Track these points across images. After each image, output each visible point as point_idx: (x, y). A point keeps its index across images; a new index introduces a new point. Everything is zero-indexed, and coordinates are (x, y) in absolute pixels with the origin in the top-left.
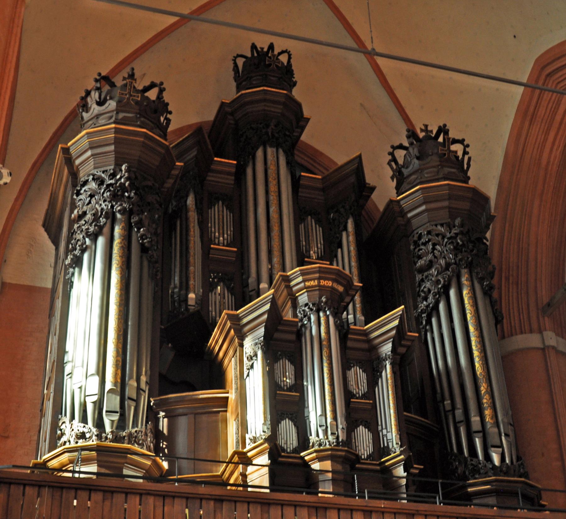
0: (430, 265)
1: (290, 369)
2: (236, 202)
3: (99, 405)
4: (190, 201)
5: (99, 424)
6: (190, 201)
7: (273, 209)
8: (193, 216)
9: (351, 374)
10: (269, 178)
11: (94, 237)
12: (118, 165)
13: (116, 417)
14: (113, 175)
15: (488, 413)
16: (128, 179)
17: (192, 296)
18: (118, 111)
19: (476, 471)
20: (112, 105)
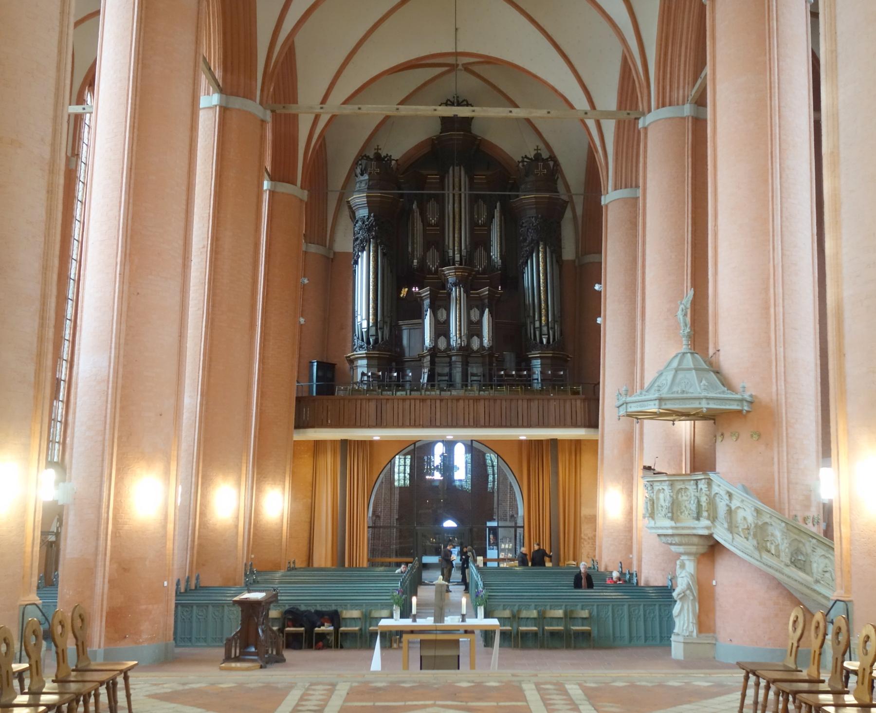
0: (525, 240)
1: (445, 312)
2: (440, 200)
3: (368, 332)
4: (414, 206)
5: (368, 342)
6: (414, 206)
7: (456, 205)
8: (417, 215)
9: (472, 312)
10: (457, 185)
11: (362, 251)
12: (370, 213)
13: (374, 338)
14: (368, 218)
15: (543, 318)
16: (375, 220)
17: (415, 261)
18: (369, 180)
19: (534, 347)
20: (366, 177)
